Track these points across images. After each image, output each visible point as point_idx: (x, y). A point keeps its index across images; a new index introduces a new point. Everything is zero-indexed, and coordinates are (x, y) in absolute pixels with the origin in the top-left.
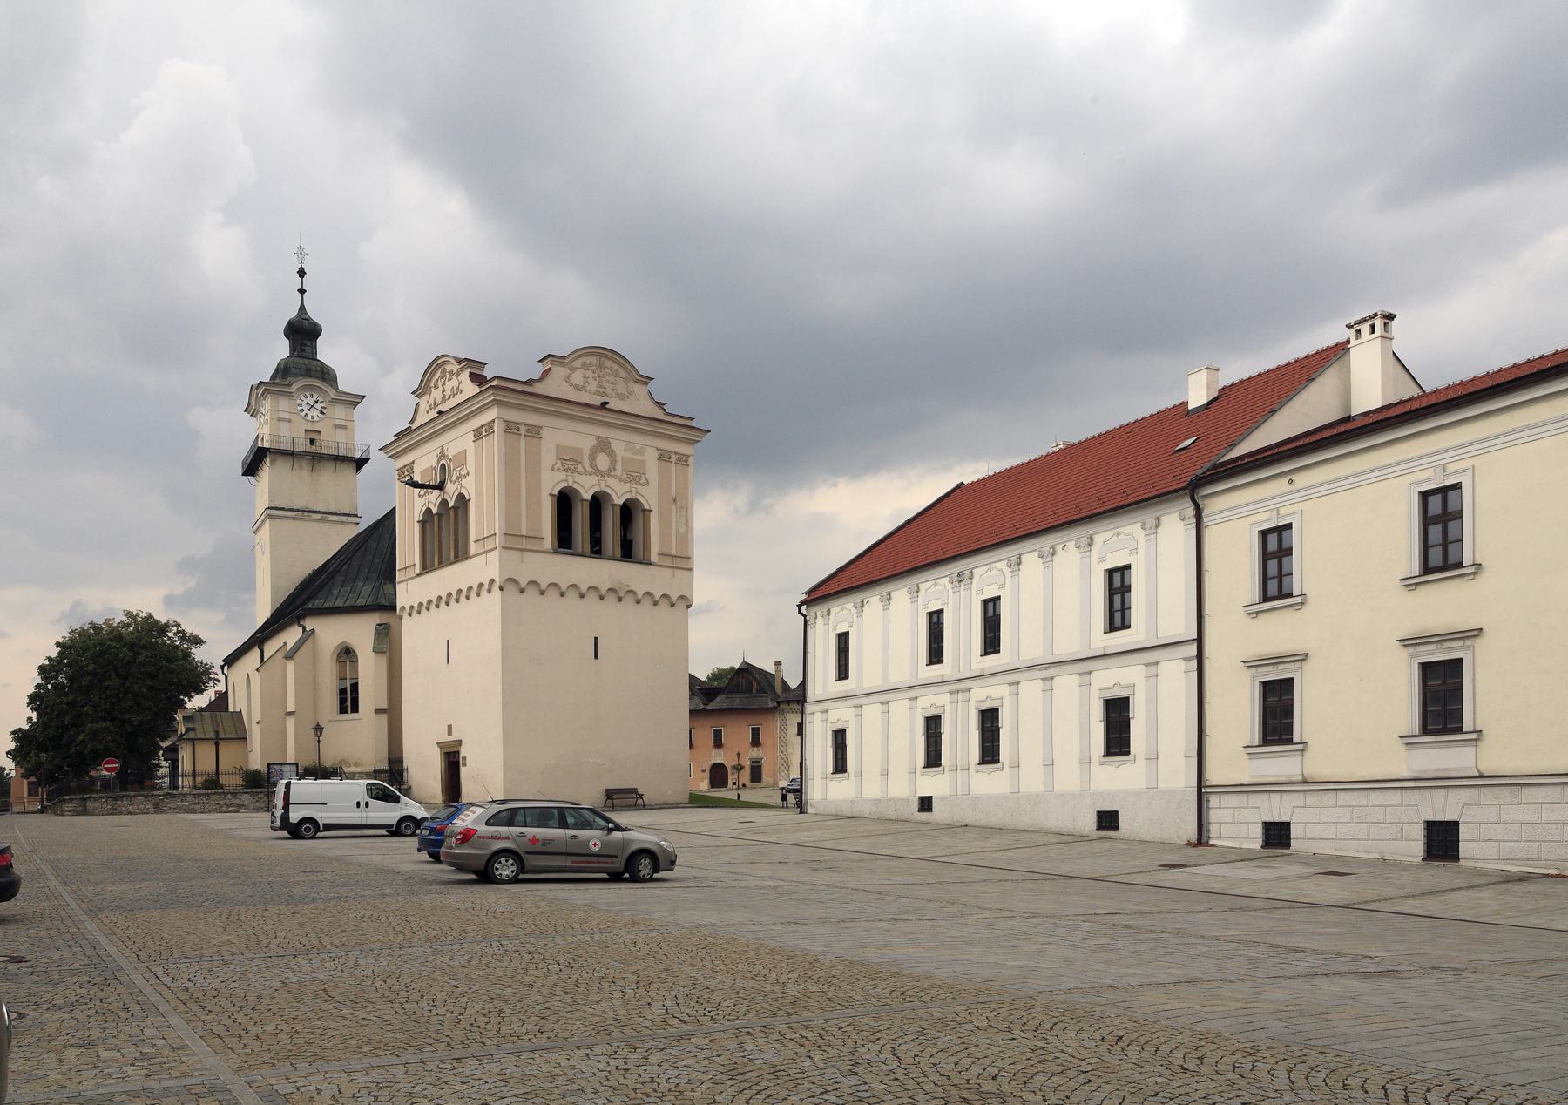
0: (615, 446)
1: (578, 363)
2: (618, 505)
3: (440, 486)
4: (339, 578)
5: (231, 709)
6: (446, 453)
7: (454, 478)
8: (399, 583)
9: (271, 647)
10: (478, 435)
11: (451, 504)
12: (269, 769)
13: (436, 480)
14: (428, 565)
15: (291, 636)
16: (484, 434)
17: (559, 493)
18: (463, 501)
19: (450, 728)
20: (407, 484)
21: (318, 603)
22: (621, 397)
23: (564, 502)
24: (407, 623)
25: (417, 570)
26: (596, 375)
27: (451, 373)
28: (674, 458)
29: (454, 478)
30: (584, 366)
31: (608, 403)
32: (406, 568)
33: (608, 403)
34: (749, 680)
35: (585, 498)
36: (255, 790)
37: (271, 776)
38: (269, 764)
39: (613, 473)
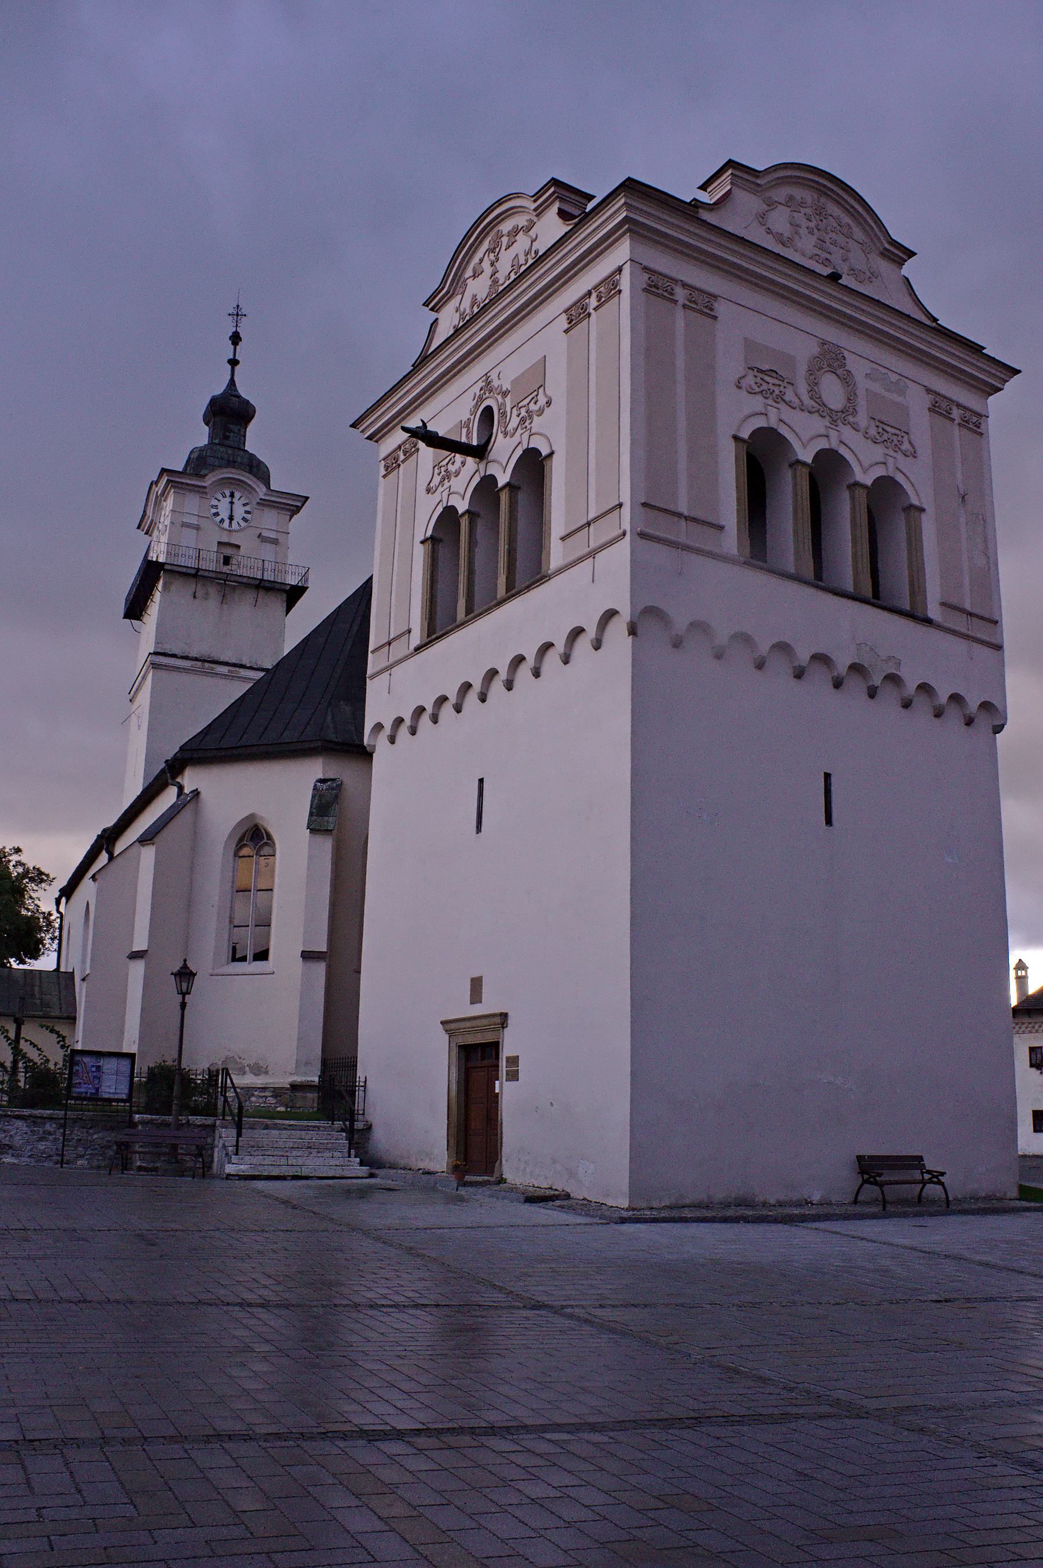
0: (857, 367)
3: (480, 452)
6: (496, 383)
26: (812, 225)
36: (37, 1112)
37: (76, 1080)
39: (851, 419)
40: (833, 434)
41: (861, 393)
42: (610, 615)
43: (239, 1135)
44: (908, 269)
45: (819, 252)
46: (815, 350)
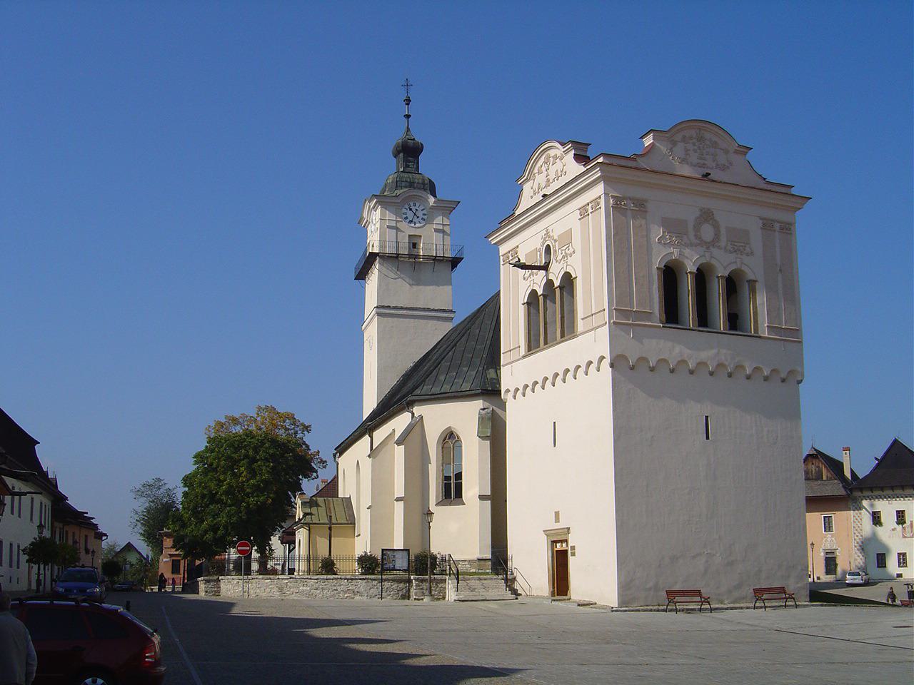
1: (679, 137)
4: (445, 364)
5: (340, 495)
6: (551, 234)
7: (560, 257)
8: (503, 366)
9: (380, 434)
10: (583, 212)
11: (557, 283)
12: (383, 554)
13: (541, 262)
14: (534, 344)
15: (400, 423)
16: (590, 211)
17: (665, 266)
18: (568, 280)
19: (557, 514)
20: (515, 266)
21: (426, 389)
22: (723, 168)
23: (670, 275)
24: (511, 405)
25: (523, 351)
27: (555, 157)
28: (777, 226)
29: (560, 257)
30: (684, 139)
31: (710, 174)
32: (510, 351)
33: (710, 174)
34: (818, 467)
38: (383, 550)
40: (707, 254)
41: (723, 231)
42: (602, 358)
43: (458, 583)
44: (750, 155)
45: (700, 161)
46: (698, 213)
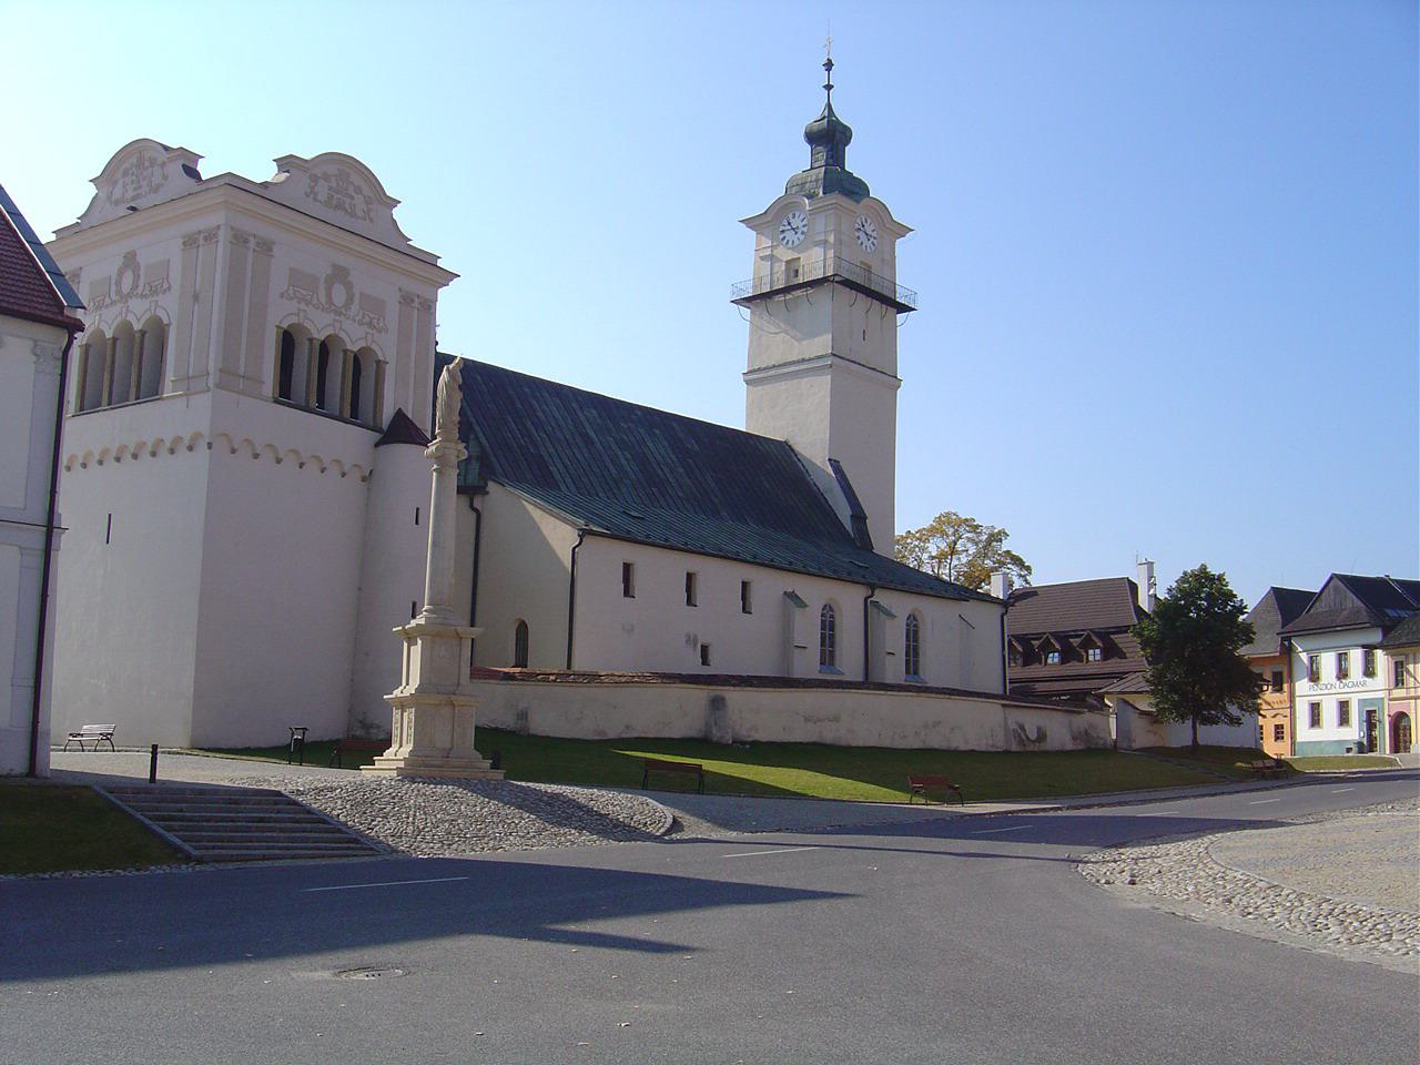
2: (352, 352)
10: (190, 242)
23: (288, 341)
35: (316, 336)
